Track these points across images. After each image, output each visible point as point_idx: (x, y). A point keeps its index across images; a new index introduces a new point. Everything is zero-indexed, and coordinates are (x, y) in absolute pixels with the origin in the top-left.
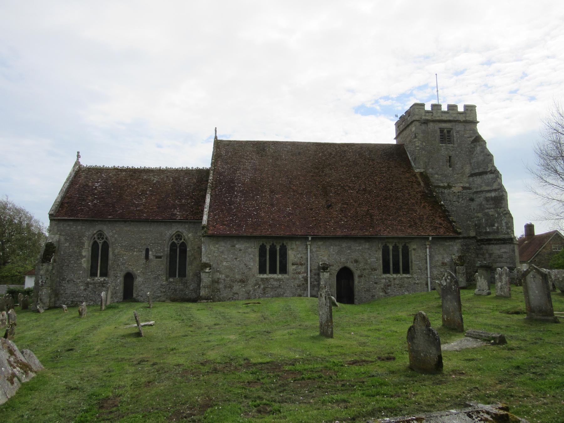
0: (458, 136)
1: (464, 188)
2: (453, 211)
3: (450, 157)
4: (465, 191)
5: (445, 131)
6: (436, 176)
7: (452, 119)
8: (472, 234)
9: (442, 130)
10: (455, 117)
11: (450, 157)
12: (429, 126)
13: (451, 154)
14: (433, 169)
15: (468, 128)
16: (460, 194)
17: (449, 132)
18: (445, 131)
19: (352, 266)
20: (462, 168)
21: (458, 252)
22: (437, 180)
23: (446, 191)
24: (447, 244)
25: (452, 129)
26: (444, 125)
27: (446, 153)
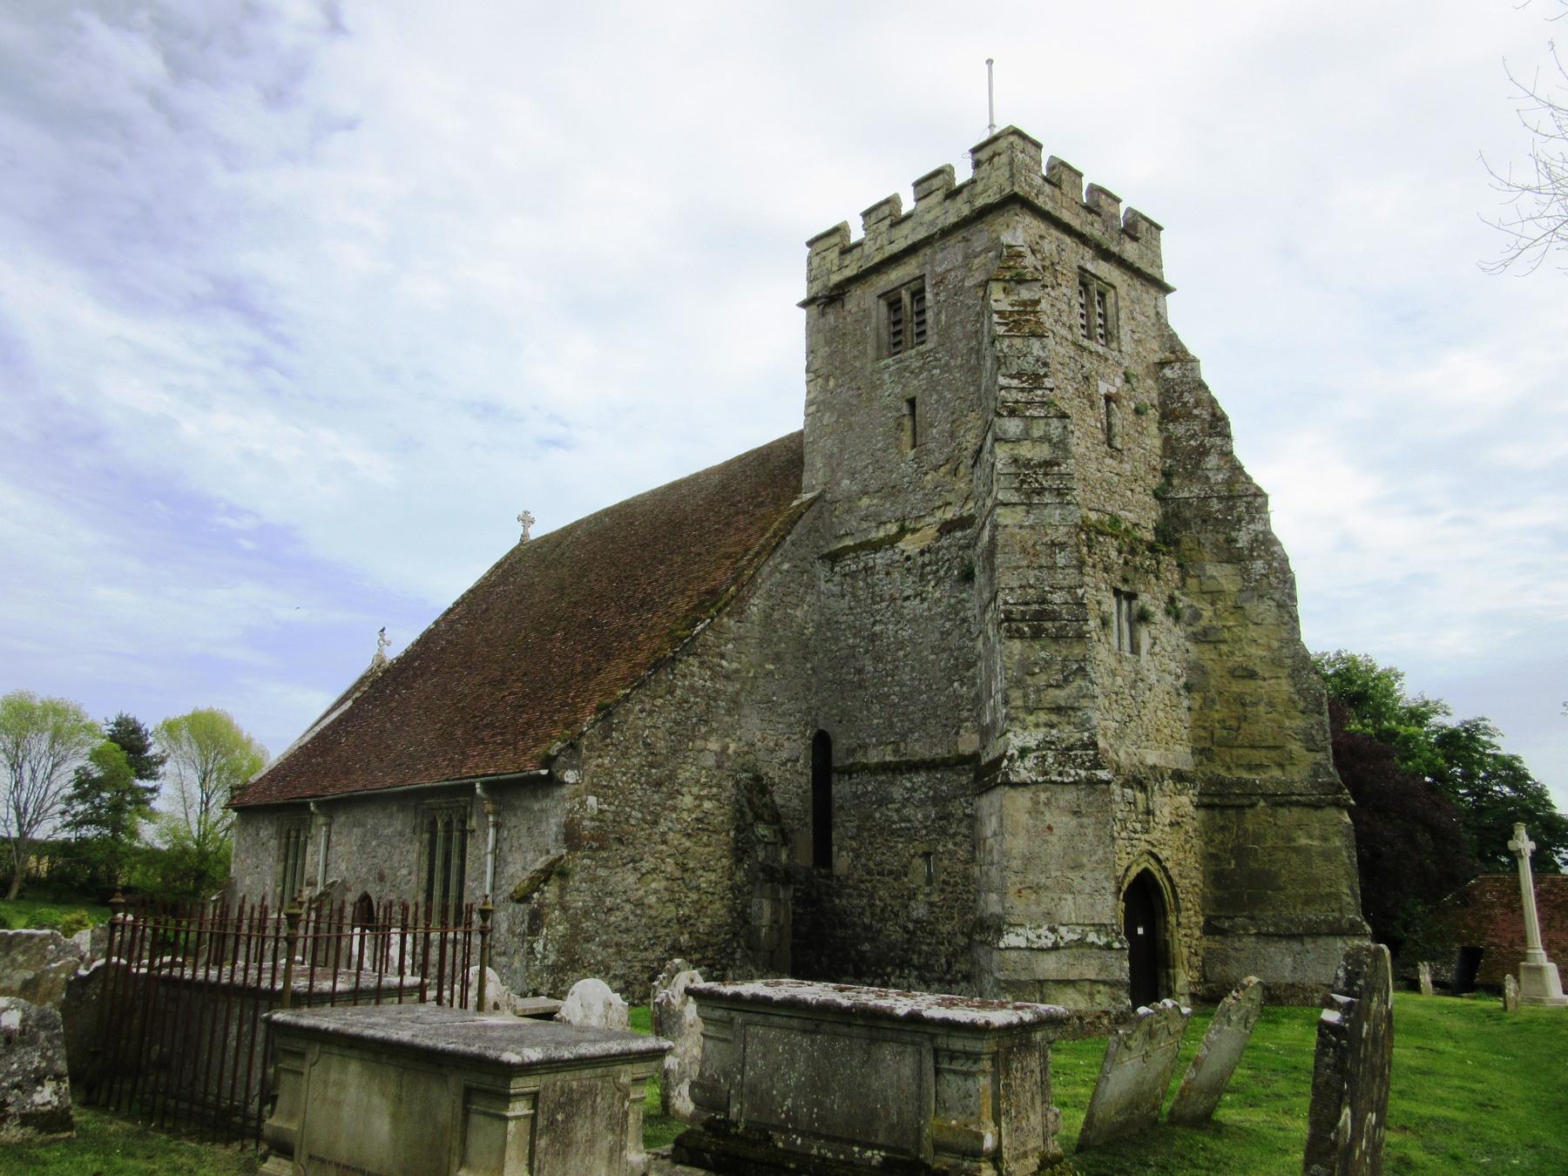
0: (942, 297)
1: (947, 528)
2: (901, 645)
3: (912, 403)
4: (945, 542)
5: (906, 297)
6: (865, 501)
7: (921, 234)
8: (968, 743)
9: (894, 304)
10: (933, 223)
11: (912, 403)
12: (848, 307)
13: (915, 385)
14: (852, 475)
15: (978, 244)
16: (927, 558)
17: (918, 295)
18: (906, 297)
19: (374, 890)
20: (952, 435)
21: (556, 840)
22: (865, 519)
23: (880, 559)
24: (536, 806)
25: (922, 277)
26: (896, 276)
27: (898, 389)
